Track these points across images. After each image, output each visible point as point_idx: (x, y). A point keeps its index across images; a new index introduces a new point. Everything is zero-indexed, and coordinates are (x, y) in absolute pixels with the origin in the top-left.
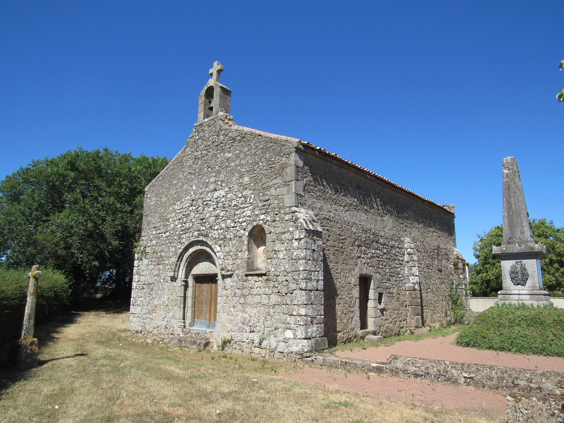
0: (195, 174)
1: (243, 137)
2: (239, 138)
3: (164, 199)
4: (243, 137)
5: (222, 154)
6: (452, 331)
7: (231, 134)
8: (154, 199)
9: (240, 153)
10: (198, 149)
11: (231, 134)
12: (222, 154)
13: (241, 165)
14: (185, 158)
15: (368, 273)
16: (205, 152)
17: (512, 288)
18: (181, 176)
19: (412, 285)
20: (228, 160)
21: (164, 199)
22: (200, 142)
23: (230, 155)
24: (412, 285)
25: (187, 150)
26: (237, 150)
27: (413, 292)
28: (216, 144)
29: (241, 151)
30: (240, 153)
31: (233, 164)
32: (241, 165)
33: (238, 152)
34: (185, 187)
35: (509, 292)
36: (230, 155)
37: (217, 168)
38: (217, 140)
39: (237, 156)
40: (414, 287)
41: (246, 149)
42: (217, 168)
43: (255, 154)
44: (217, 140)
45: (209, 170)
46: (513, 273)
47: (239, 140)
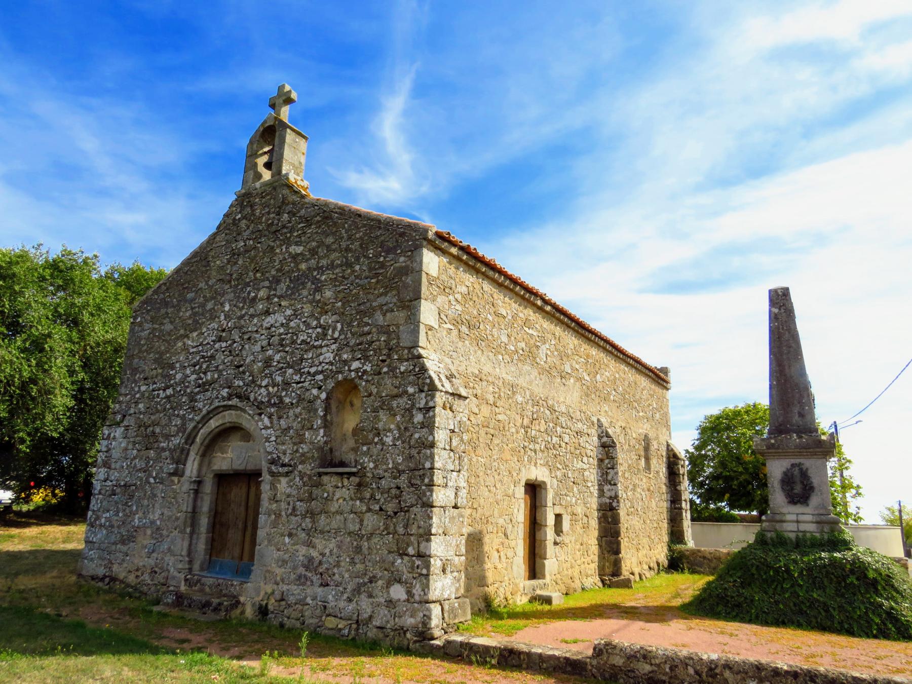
0: (230, 282)
1: (327, 218)
2: (318, 218)
3: (168, 327)
4: (327, 218)
5: (284, 248)
6: (604, 565)
7: (303, 212)
8: (146, 326)
9: (318, 247)
10: (239, 238)
11: (303, 212)
12: (284, 248)
13: (319, 269)
14: (212, 253)
15: (540, 478)
16: (251, 242)
17: (784, 510)
18: (202, 285)
19: (608, 501)
20: (295, 257)
21: (168, 327)
22: (243, 224)
23: (299, 249)
24: (608, 501)
25: (218, 239)
26: (313, 240)
27: (610, 513)
28: (274, 228)
29: (321, 244)
30: (318, 247)
31: (303, 266)
32: (319, 269)
33: (314, 244)
34: (209, 306)
35: (778, 517)
36: (299, 249)
37: (273, 272)
38: (276, 222)
39: (313, 252)
40: (610, 503)
41: (330, 240)
42: (273, 272)
43: (348, 250)
44: (276, 222)
45: (258, 275)
46: (787, 481)
47: (318, 222)
